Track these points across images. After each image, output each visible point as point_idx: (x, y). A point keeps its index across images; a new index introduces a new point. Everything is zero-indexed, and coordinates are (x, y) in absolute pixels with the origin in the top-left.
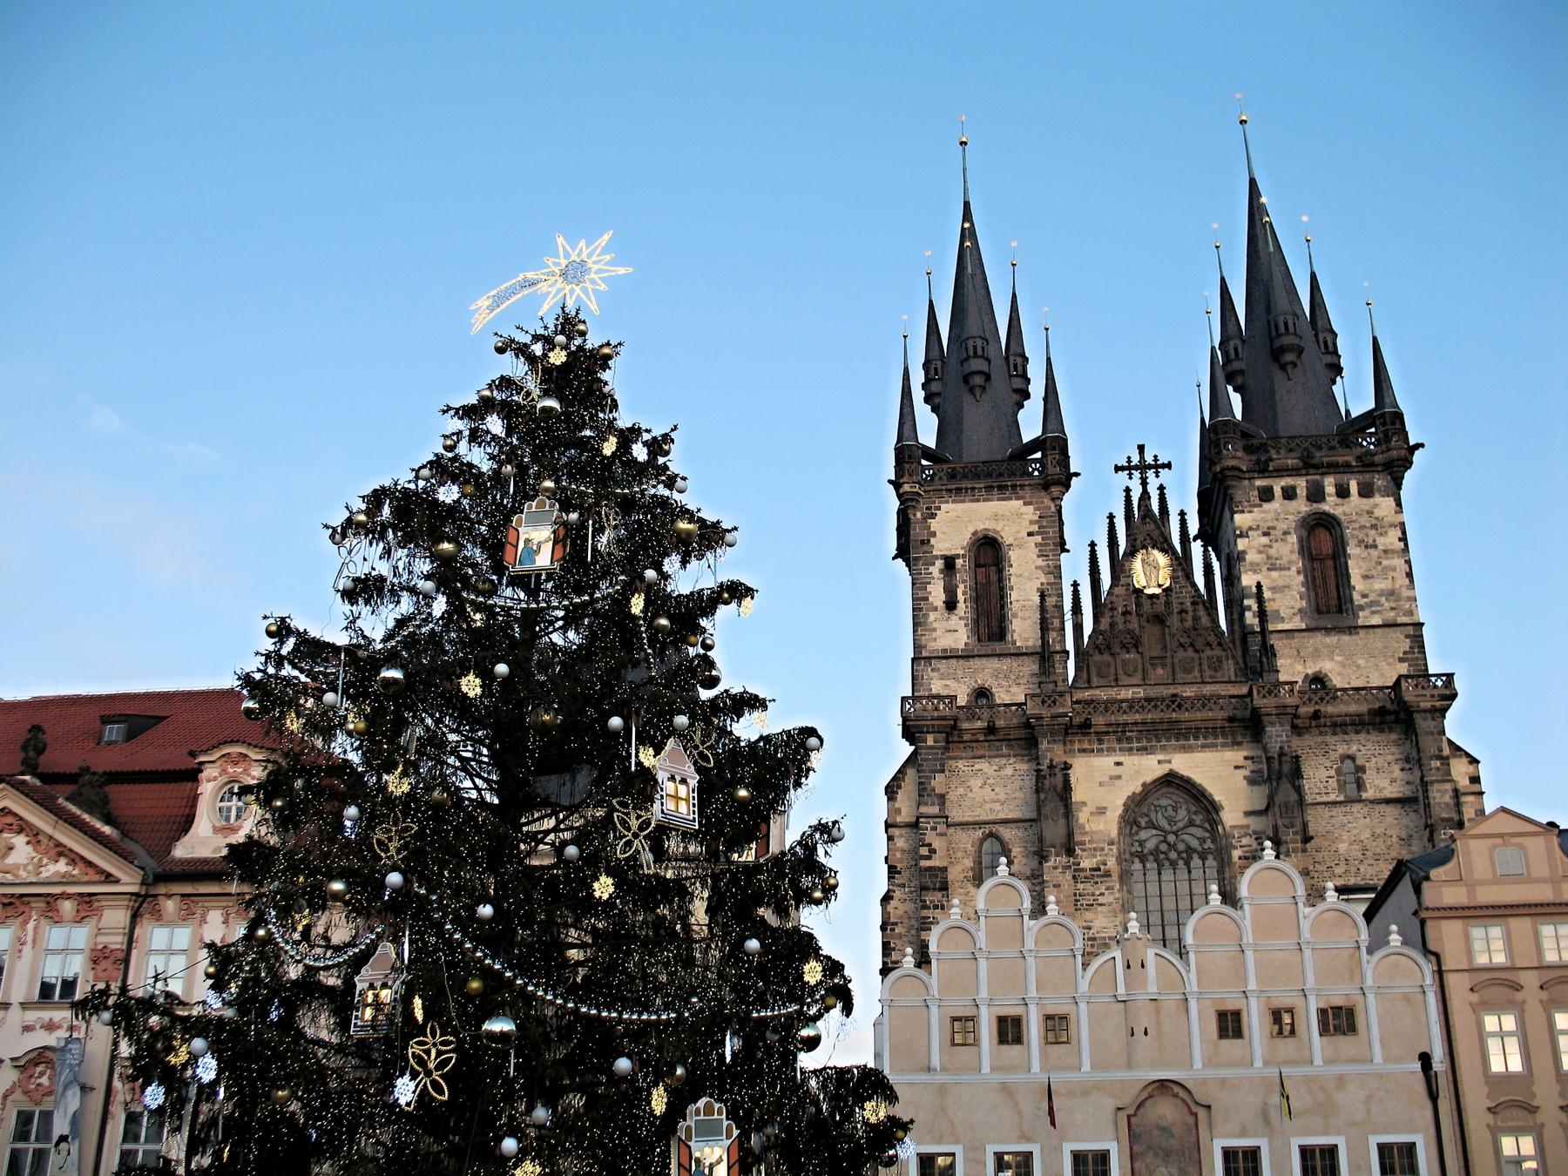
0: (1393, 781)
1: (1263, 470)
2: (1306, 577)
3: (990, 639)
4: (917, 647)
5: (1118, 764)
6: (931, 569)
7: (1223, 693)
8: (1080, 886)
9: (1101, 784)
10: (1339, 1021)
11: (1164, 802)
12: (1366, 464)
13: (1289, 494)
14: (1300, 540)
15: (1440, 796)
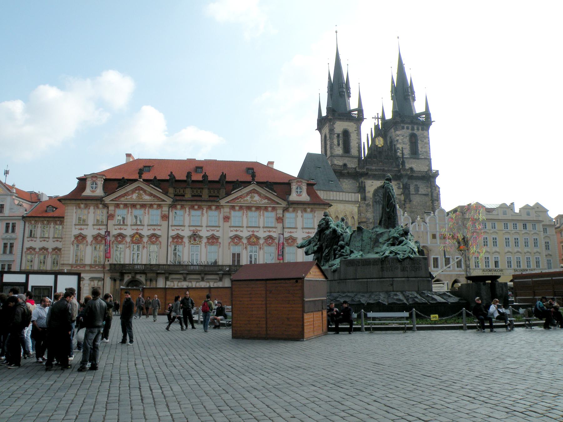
0: (424, 190)
1: (403, 122)
4: (331, 153)
5: (372, 182)
6: (334, 136)
7: (393, 169)
9: (369, 186)
11: (380, 191)
13: (408, 128)
15: (435, 195)
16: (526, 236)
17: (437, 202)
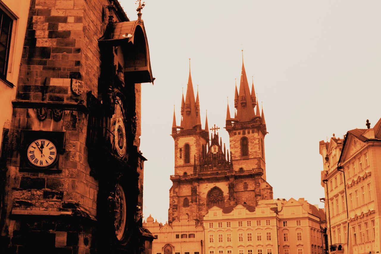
0: (253, 187)
2: (241, 149)
3: (188, 163)
4: (175, 165)
5: (207, 185)
8: (200, 207)
9: (204, 189)
10: (191, 236)
12: (253, 127)
13: (239, 133)
14: (241, 142)
16: (259, 231)
17: (259, 197)
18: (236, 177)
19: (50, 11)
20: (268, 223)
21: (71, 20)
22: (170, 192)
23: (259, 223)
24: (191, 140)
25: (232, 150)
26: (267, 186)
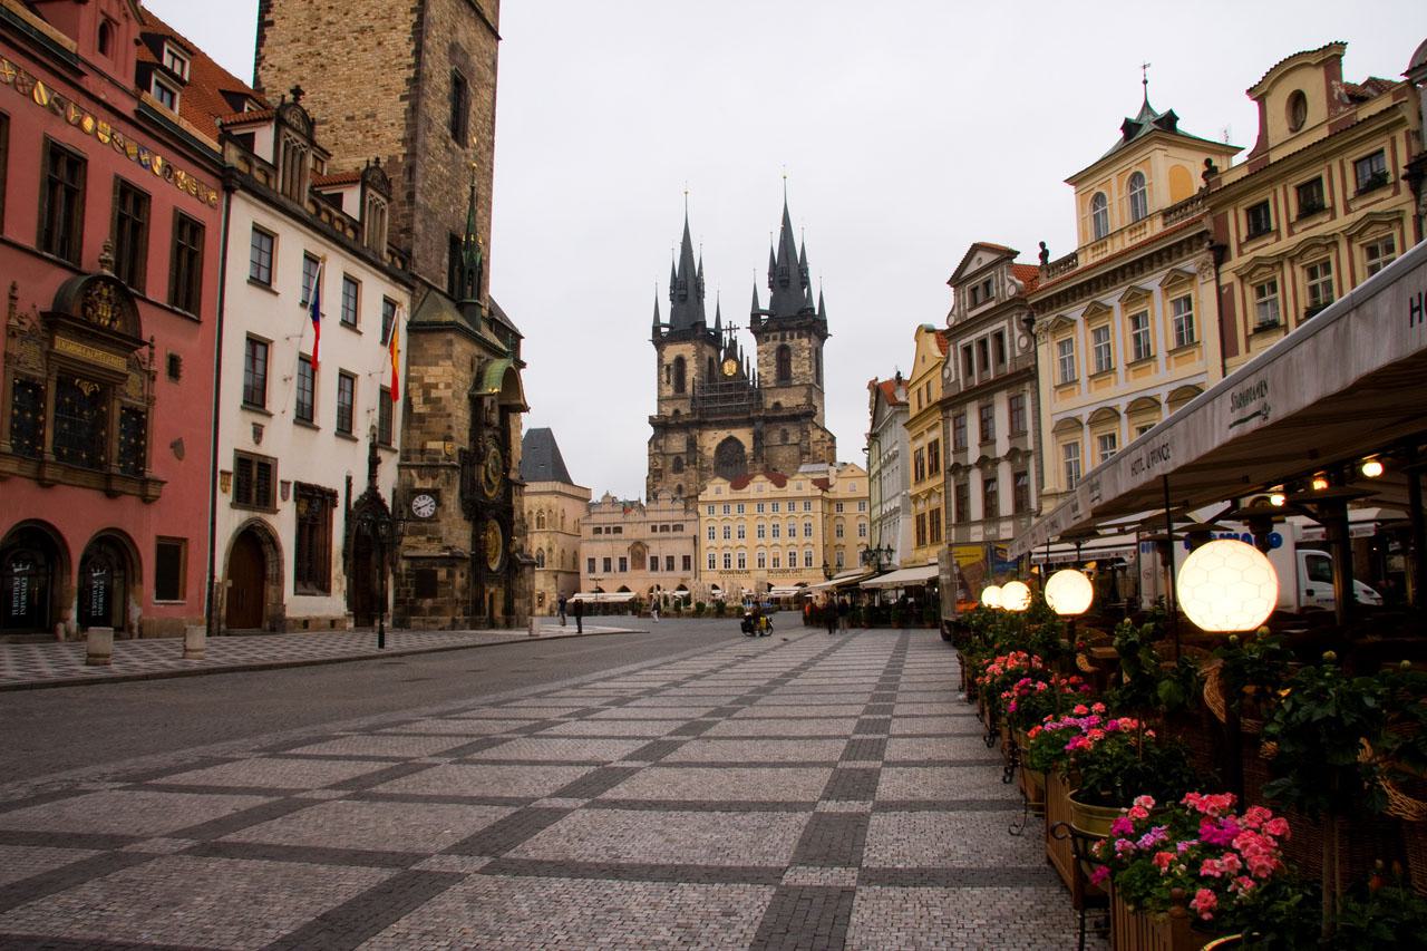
12: (799, 328)
13: (775, 339)
16: (791, 521)
18: (767, 420)
19: (423, 377)
20: (807, 506)
21: (441, 386)
22: (649, 446)
23: (792, 507)
24: (687, 350)
25: (761, 369)
26: (822, 437)
